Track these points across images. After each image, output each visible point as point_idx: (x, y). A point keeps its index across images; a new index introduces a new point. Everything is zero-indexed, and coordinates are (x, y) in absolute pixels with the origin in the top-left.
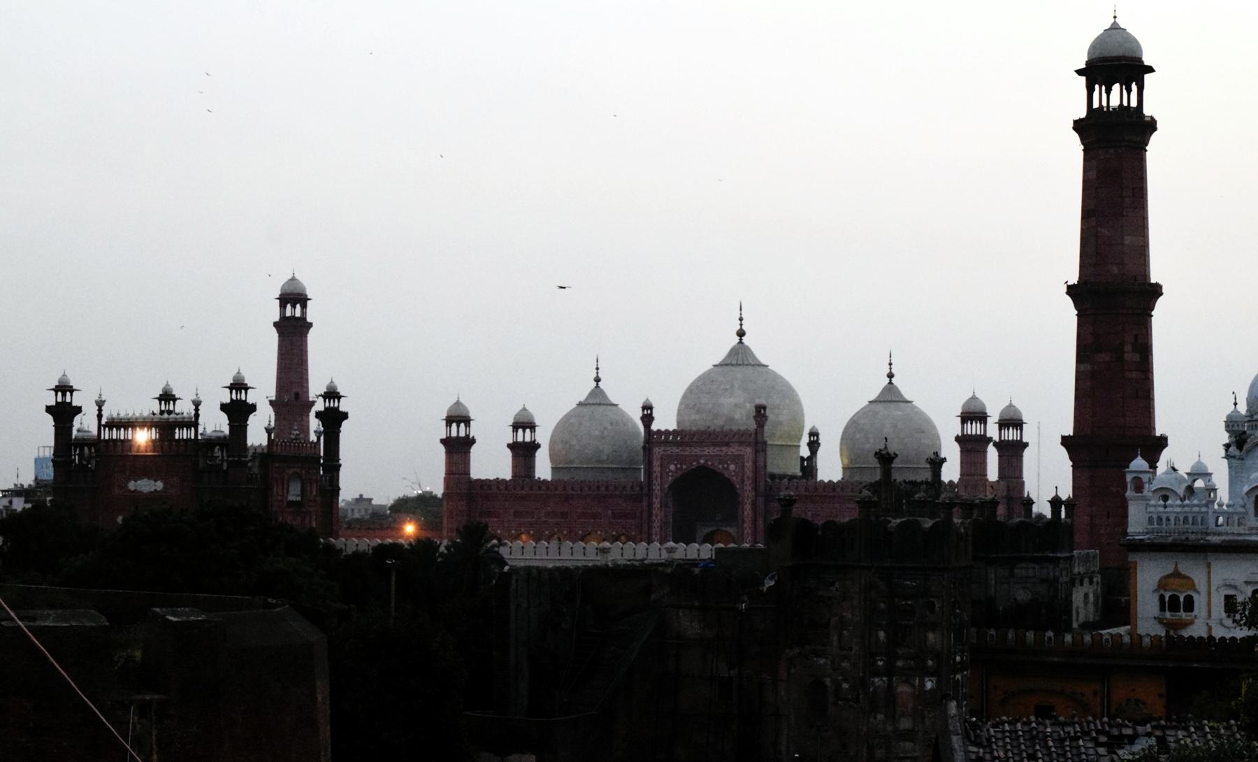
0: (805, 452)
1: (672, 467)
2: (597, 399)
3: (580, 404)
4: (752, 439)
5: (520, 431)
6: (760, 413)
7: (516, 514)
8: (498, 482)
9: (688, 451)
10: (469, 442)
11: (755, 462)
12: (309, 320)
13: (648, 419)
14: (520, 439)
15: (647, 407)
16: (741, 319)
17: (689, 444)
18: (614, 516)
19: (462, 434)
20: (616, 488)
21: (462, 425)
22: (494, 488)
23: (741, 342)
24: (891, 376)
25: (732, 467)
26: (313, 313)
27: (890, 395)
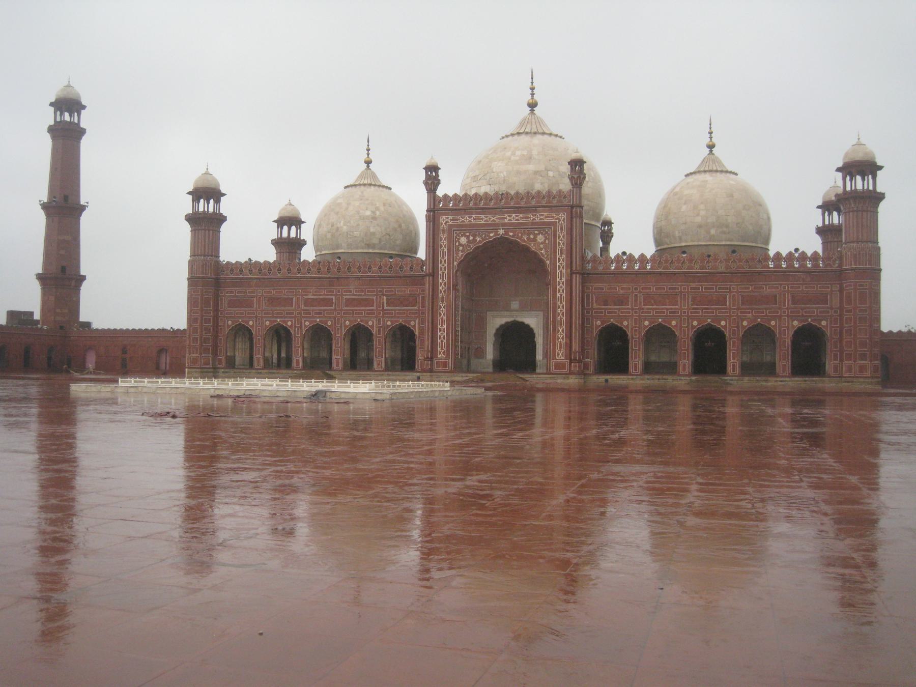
1: (463, 240)
2: (368, 181)
5: (285, 228)
7: (272, 302)
8: (251, 265)
9: (484, 219)
10: (218, 220)
12: (82, 125)
14: (285, 234)
17: (484, 210)
18: (390, 302)
19: (211, 210)
21: (212, 201)
23: (532, 111)
25: (540, 238)
26: (86, 120)
27: (711, 166)
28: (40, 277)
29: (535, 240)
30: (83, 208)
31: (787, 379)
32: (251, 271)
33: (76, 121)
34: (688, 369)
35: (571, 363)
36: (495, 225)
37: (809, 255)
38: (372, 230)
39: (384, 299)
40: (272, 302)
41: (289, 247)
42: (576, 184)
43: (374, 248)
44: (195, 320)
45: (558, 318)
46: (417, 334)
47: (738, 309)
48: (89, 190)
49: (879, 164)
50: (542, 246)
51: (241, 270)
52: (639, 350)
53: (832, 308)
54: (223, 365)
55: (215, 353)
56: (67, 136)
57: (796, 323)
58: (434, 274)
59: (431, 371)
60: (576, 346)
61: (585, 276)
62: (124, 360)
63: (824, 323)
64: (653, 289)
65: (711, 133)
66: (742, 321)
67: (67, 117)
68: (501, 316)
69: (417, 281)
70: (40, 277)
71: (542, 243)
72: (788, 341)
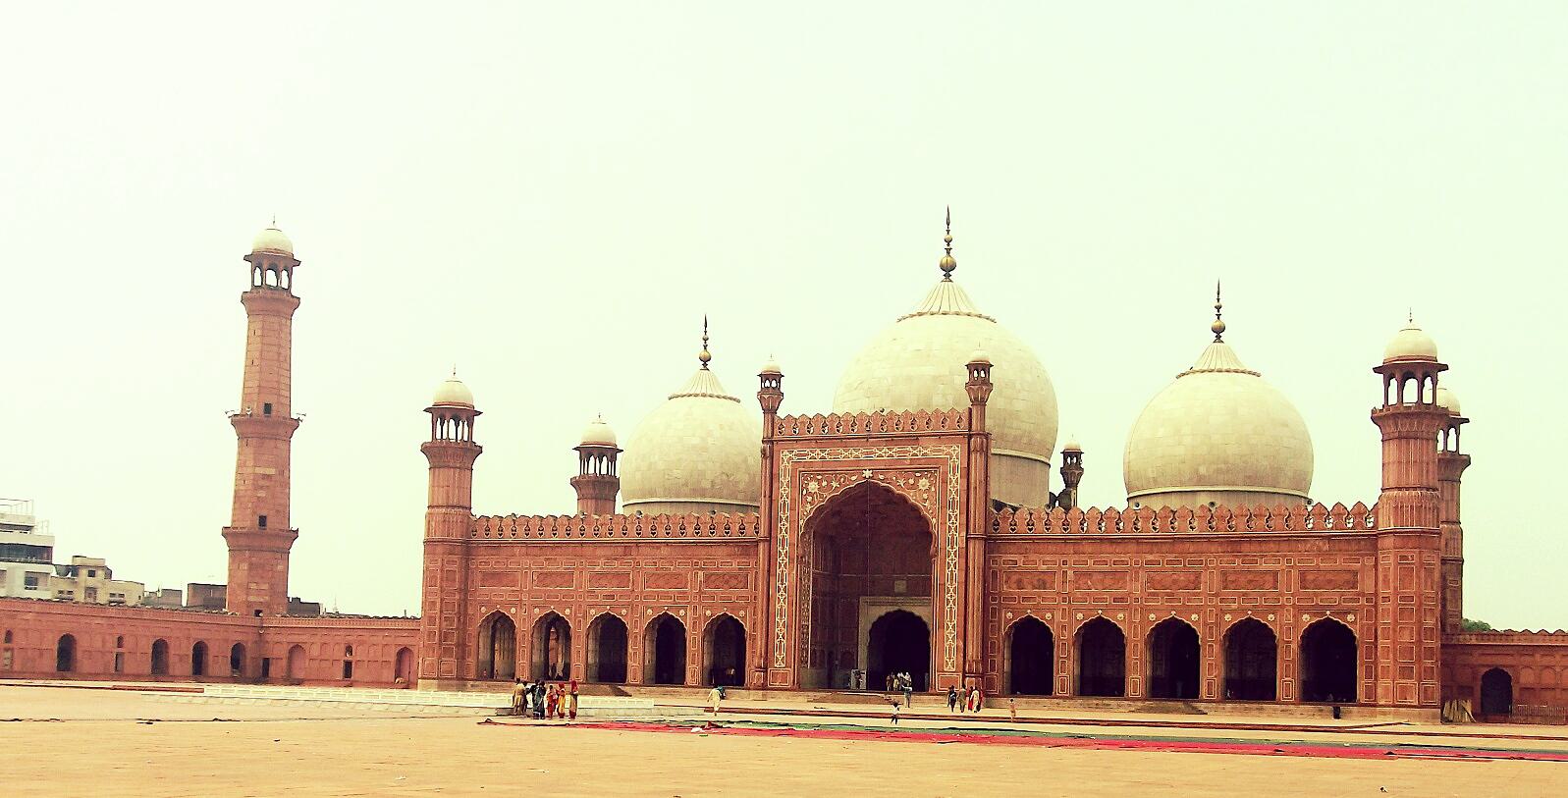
1: (813, 486)
4: (964, 427)
17: (843, 441)
20: (713, 528)
22: (507, 532)
25: (923, 483)
28: (227, 533)
29: (914, 486)
31: (1292, 707)
34: (1141, 691)
35: (964, 677)
36: (858, 461)
38: (701, 466)
40: (544, 577)
41: (598, 489)
42: (976, 399)
43: (703, 496)
44: (434, 603)
45: (947, 608)
47: (1216, 595)
50: (925, 496)
52: (1068, 658)
53: (1364, 595)
54: (472, 675)
55: (462, 657)
57: (1307, 619)
58: (769, 539)
59: (764, 687)
60: (973, 651)
61: (992, 543)
62: (348, 665)
63: (1350, 618)
64: (1090, 562)
66: (1224, 612)
68: (881, 604)
69: (747, 547)
70: (227, 533)
71: (925, 491)
72: (1294, 646)
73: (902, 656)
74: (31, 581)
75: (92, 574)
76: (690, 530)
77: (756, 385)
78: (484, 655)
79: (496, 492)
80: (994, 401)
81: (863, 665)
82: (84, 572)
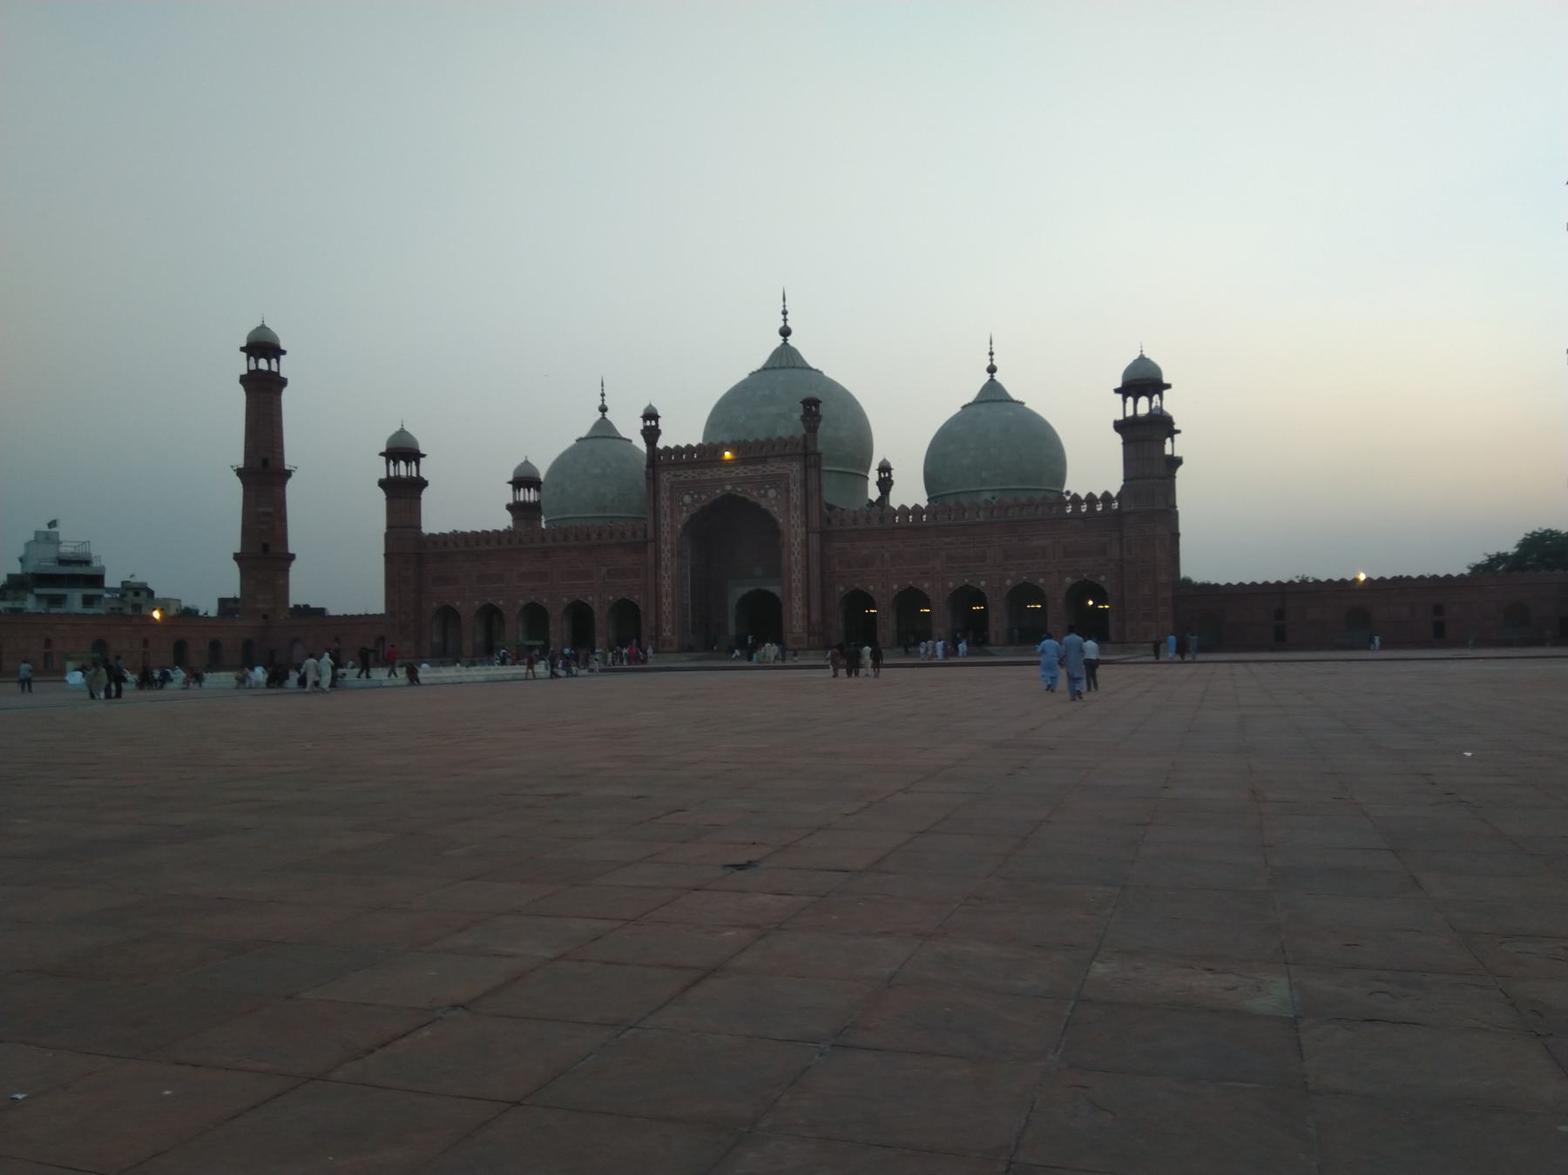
0: (874, 493)
1: (687, 499)
2: (604, 431)
3: (579, 440)
6: (811, 408)
8: (458, 539)
10: (420, 484)
11: (805, 483)
13: (651, 434)
15: (651, 415)
16: (785, 313)
20: (611, 534)
24: (992, 370)
25: (772, 493)
26: (286, 366)
27: (993, 394)
29: (765, 496)
30: (288, 474)
32: (456, 545)
33: (274, 368)
37: (1099, 496)
39: (604, 570)
46: (642, 608)
48: (294, 452)
49: (1165, 380)
51: (445, 544)
56: (263, 391)
57: (1069, 580)
60: (815, 616)
63: (1103, 578)
65: (991, 354)
67: (263, 364)
70: (237, 557)
73: (760, 625)
74: (88, 601)
75: (137, 594)
76: (594, 536)
77: (640, 425)
78: (436, 639)
79: (440, 515)
80: (824, 430)
81: (732, 630)
82: (130, 594)
